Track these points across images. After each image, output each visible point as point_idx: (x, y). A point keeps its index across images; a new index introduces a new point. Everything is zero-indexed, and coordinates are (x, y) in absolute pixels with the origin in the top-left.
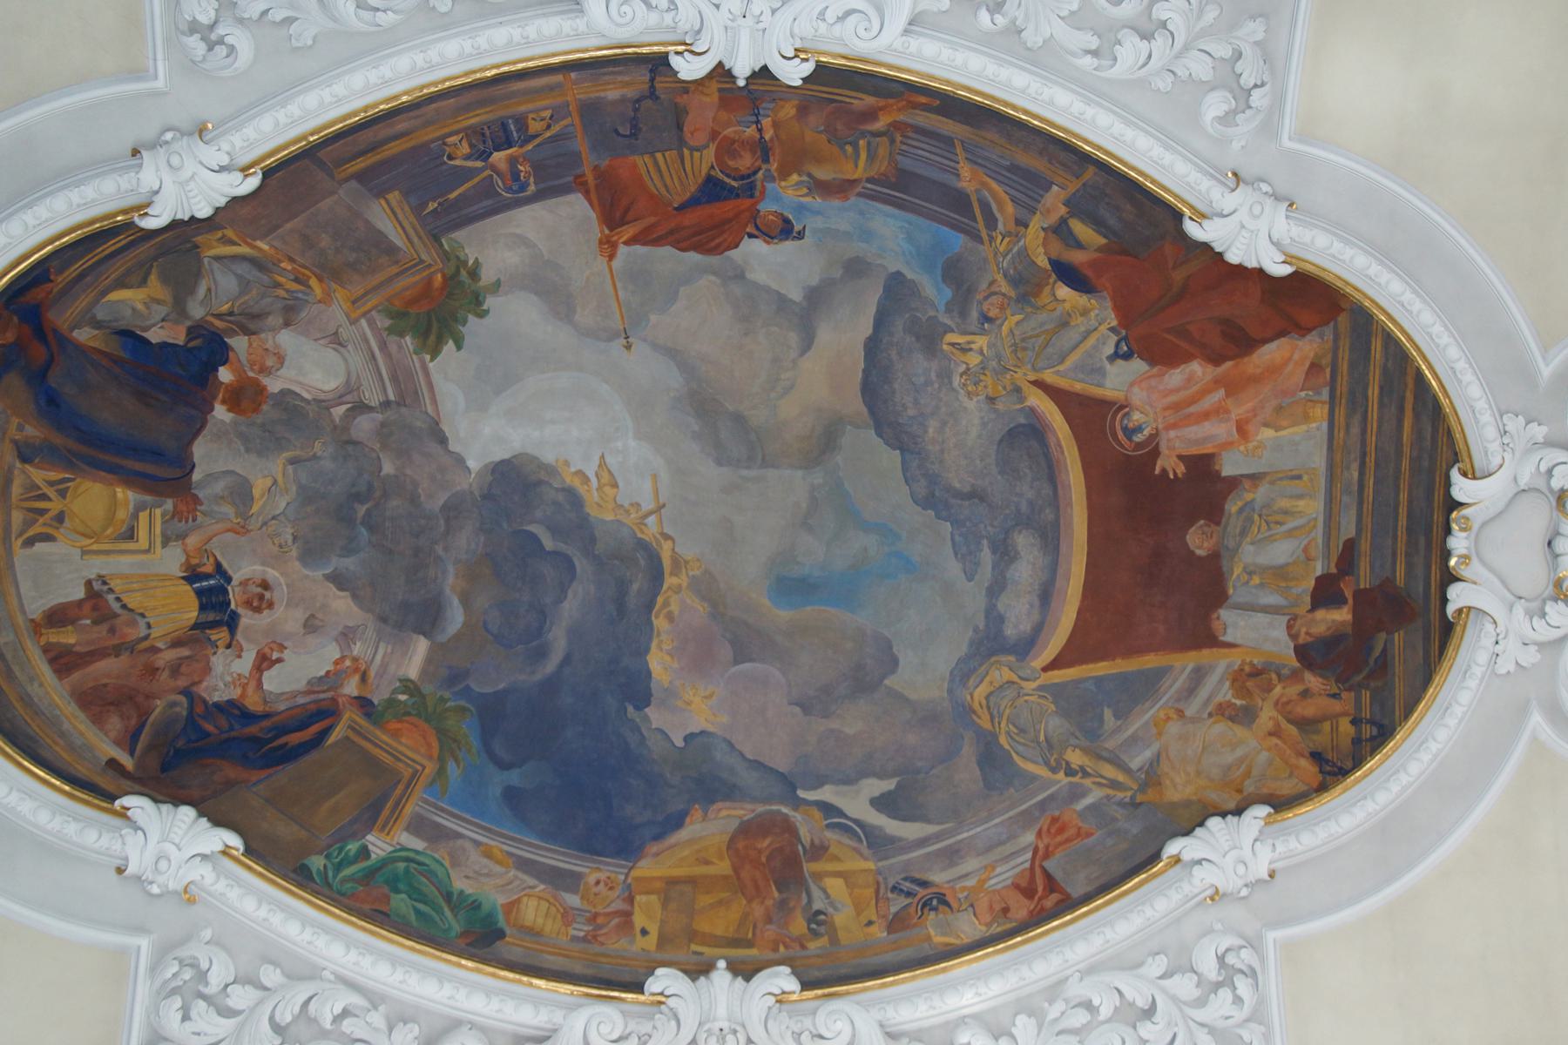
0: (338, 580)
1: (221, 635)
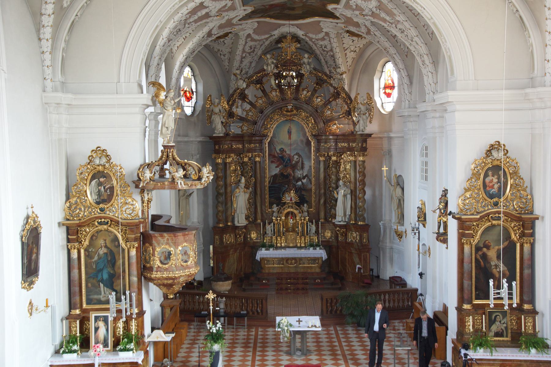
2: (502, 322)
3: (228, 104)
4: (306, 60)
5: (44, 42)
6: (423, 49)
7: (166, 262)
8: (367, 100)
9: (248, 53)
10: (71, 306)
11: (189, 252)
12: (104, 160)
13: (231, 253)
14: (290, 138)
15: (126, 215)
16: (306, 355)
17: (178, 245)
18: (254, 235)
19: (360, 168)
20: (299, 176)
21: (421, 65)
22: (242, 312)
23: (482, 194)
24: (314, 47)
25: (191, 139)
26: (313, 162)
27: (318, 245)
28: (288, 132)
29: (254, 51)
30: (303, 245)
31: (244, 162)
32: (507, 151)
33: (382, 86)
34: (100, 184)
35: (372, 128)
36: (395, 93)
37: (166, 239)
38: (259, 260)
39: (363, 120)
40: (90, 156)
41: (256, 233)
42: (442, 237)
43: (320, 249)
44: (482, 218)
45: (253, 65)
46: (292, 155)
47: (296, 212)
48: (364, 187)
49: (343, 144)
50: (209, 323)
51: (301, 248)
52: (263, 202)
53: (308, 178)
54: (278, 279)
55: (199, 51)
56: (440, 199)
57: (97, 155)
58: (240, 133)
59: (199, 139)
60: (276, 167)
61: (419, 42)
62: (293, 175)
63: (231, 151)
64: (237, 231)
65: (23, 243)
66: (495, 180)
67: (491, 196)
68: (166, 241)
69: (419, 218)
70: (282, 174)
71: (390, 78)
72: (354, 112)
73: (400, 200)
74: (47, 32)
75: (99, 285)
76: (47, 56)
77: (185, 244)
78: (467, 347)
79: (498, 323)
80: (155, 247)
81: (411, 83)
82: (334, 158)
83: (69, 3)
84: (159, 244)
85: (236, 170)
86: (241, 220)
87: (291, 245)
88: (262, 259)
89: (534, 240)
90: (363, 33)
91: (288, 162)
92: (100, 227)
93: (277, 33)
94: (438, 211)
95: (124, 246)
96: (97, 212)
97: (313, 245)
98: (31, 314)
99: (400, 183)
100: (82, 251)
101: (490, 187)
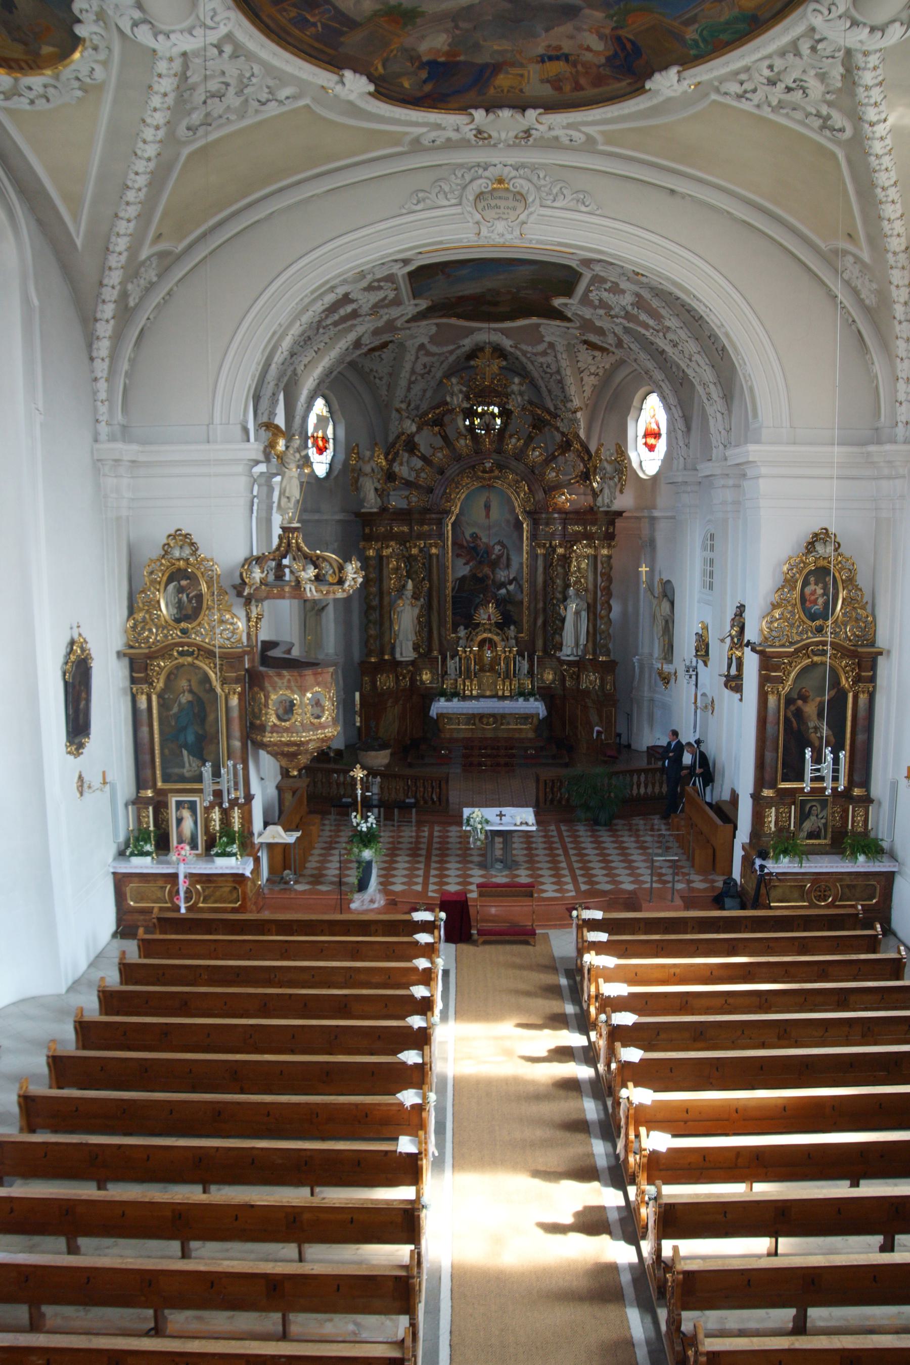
0: (547, 30)
1: (572, 58)
2: (820, 816)
3: (386, 458)
4: (515, 388)
5: (98, 363)
6: (708, 375)
7: (286, 717)
8: (615, 455)
9: (420, 374)
10: (140, 784)
11: (322, 702)
12: (187, 551)
13: (389, 704)
14: (488, 516)
15: (221, 640)
16: (510, 868)
17: (306, 691)
18: (426, 677)
19: (603, 568)
20: (503, 579)
21: (705, 401)
22: (407, 801)
23: (799, 614)
24: (530, 367)
25: (325, 517)
27: (531, 694)
28: (485, 506)
29: (430, 371)
31: (411, 555)
32: (839, 544)
33: (641, 433)
34: (180, 590)
35: (624, 501)
36: (662, 445)
37: (285, 681)
38: (435, 717)
39: (609, 488)
40: (165, 545)
41: (431, 672)
42: (734, 683)
43: (536, 700)
44: (797, 651)
45: (429, 394)
46: (492, 544)
47: (496, 638)
48: (610, 598)
49: (576, 528)
50: (355, 817)
51: (503, 698)
52: (442, 623)
54: (466, 748)
55: (339, 373)
56: (733, 620)
57: (176, 543)
58: (406, 507)
59: (338, 517)
60: (465, 564)
61: (702, 363)
63: (389, 536)
64: (399, 669)
65: (66, 683)
66: (820, 591)
67: (813, 617)
68: (285, 684)
69: (697, 651)
70: (473, 577)
71: (653, 421)
72: (595, 475)
73: (667, 622)
74: (103, 348)
75: (181, 752)
76: (102, 385)
77: (317, 689)
78: (764, 855)
79: (813, 818)
80: (269, 692)
81: (689, 428)
82: (560, 551)
83: (137, 301)
84: (274, 688)
85: (398, 568)
86: (406, 652)
87: (488, 693)
88: (441, 716)
89: (874, 687)
90: (610, 345)
91: (485, 555)
92: (181, 660)
93: (468, 343)
94: (728, 640)
95: (219, 690)
96: (177, 635)
97: (523, 694)
98: (81, 794)
99: (667, 593)
100: (154, 698)
101: (811, 602)
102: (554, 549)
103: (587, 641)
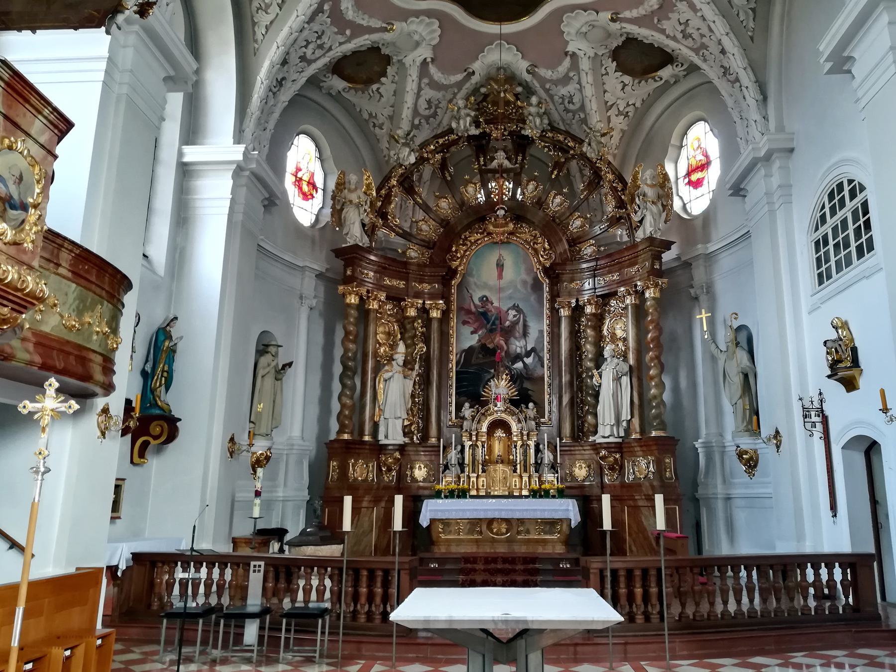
3: (377, 193)
4: (533, 110)
14: (500, 276)
20: (519, 350)
26: (546, 322)
28: (497, 265)
29: (435, 115)
30: (525, 493)
46: (505, 309)
49: (609, 278)
53: (537, 354)
60: (472, 333)
62: (505, 348)
91: (497, 322)
102: (578, 310)
103: (632, 416)
